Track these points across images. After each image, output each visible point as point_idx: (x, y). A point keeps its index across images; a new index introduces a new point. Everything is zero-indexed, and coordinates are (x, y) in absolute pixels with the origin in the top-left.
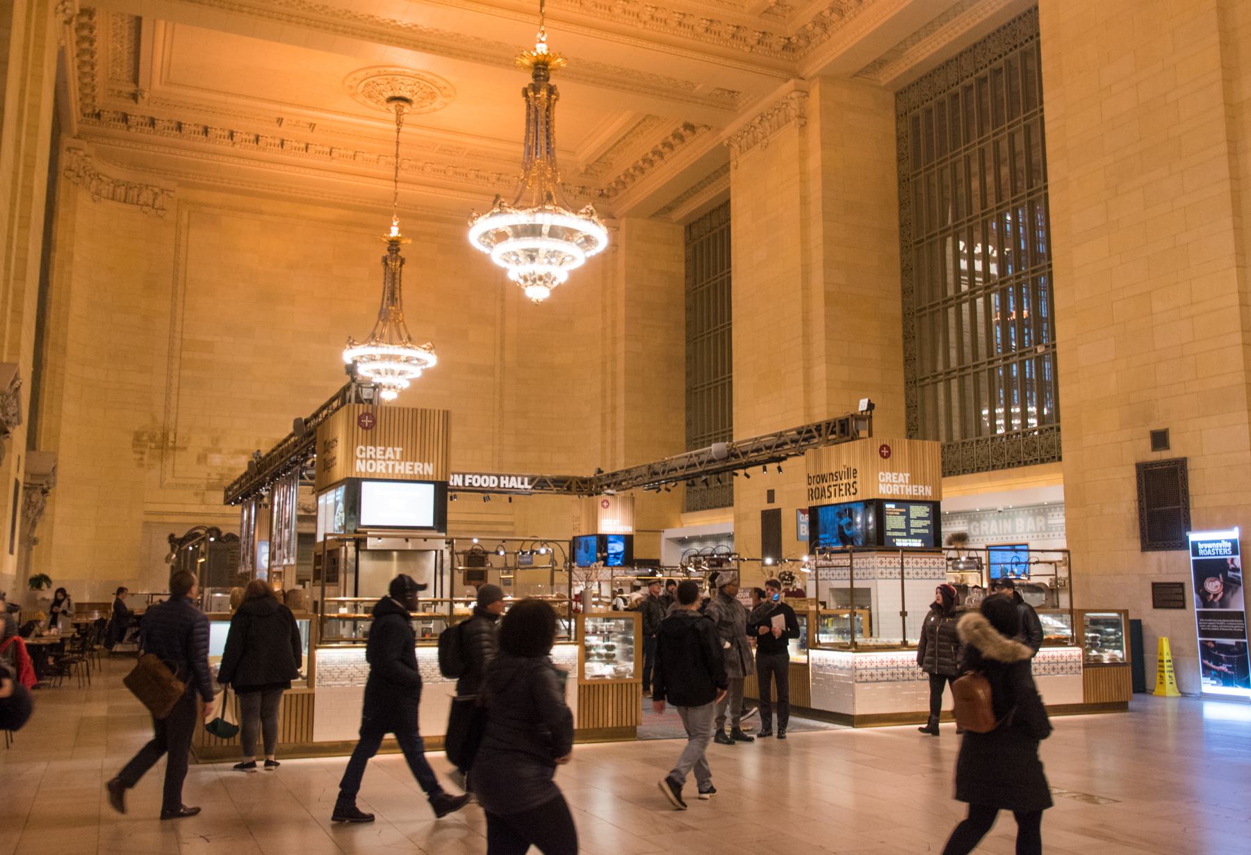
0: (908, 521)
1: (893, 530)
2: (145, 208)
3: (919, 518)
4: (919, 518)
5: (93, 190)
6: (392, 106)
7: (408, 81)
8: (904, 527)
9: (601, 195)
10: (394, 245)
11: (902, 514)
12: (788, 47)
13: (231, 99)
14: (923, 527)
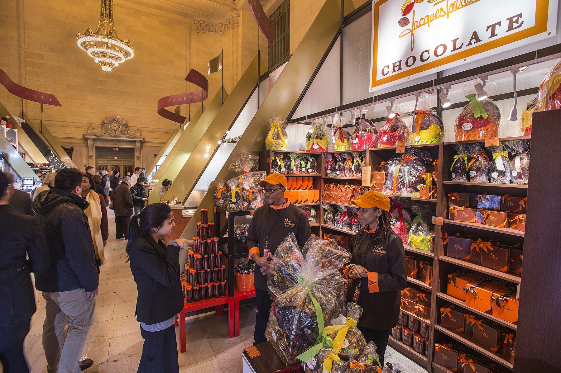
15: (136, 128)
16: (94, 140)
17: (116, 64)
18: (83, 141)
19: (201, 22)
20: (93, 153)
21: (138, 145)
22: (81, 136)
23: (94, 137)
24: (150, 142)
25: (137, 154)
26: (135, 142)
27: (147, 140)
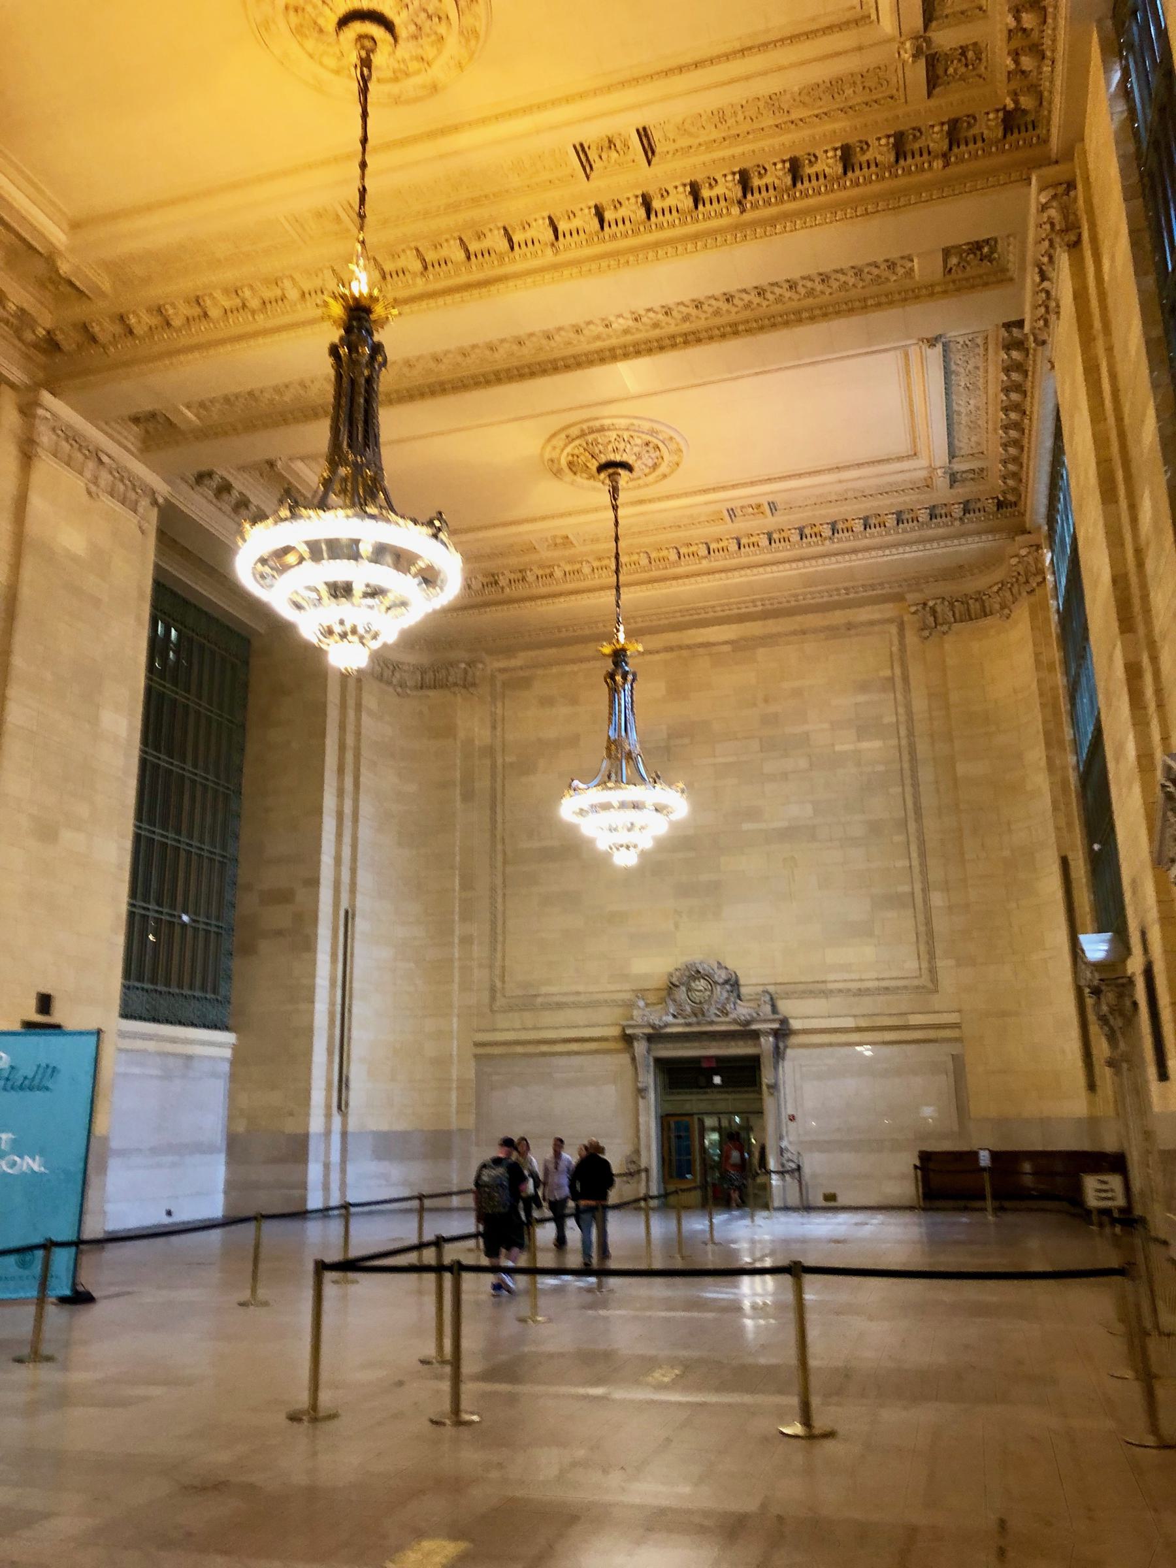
2: (456, 689)
5: (395, 681)
12: (1011, 121)
15: (760, 989)
16: (650, 1038)
17: (647, 843)
18: (620, 1045)
19: (931, 603)
20: (648, 1079)
21: (768, 1042)
22: (615, 1031)
23: (650, 1031)
24: (806, 1032)
25: (767, 1078)
26: (755, 1035)
27: (795, 1024)
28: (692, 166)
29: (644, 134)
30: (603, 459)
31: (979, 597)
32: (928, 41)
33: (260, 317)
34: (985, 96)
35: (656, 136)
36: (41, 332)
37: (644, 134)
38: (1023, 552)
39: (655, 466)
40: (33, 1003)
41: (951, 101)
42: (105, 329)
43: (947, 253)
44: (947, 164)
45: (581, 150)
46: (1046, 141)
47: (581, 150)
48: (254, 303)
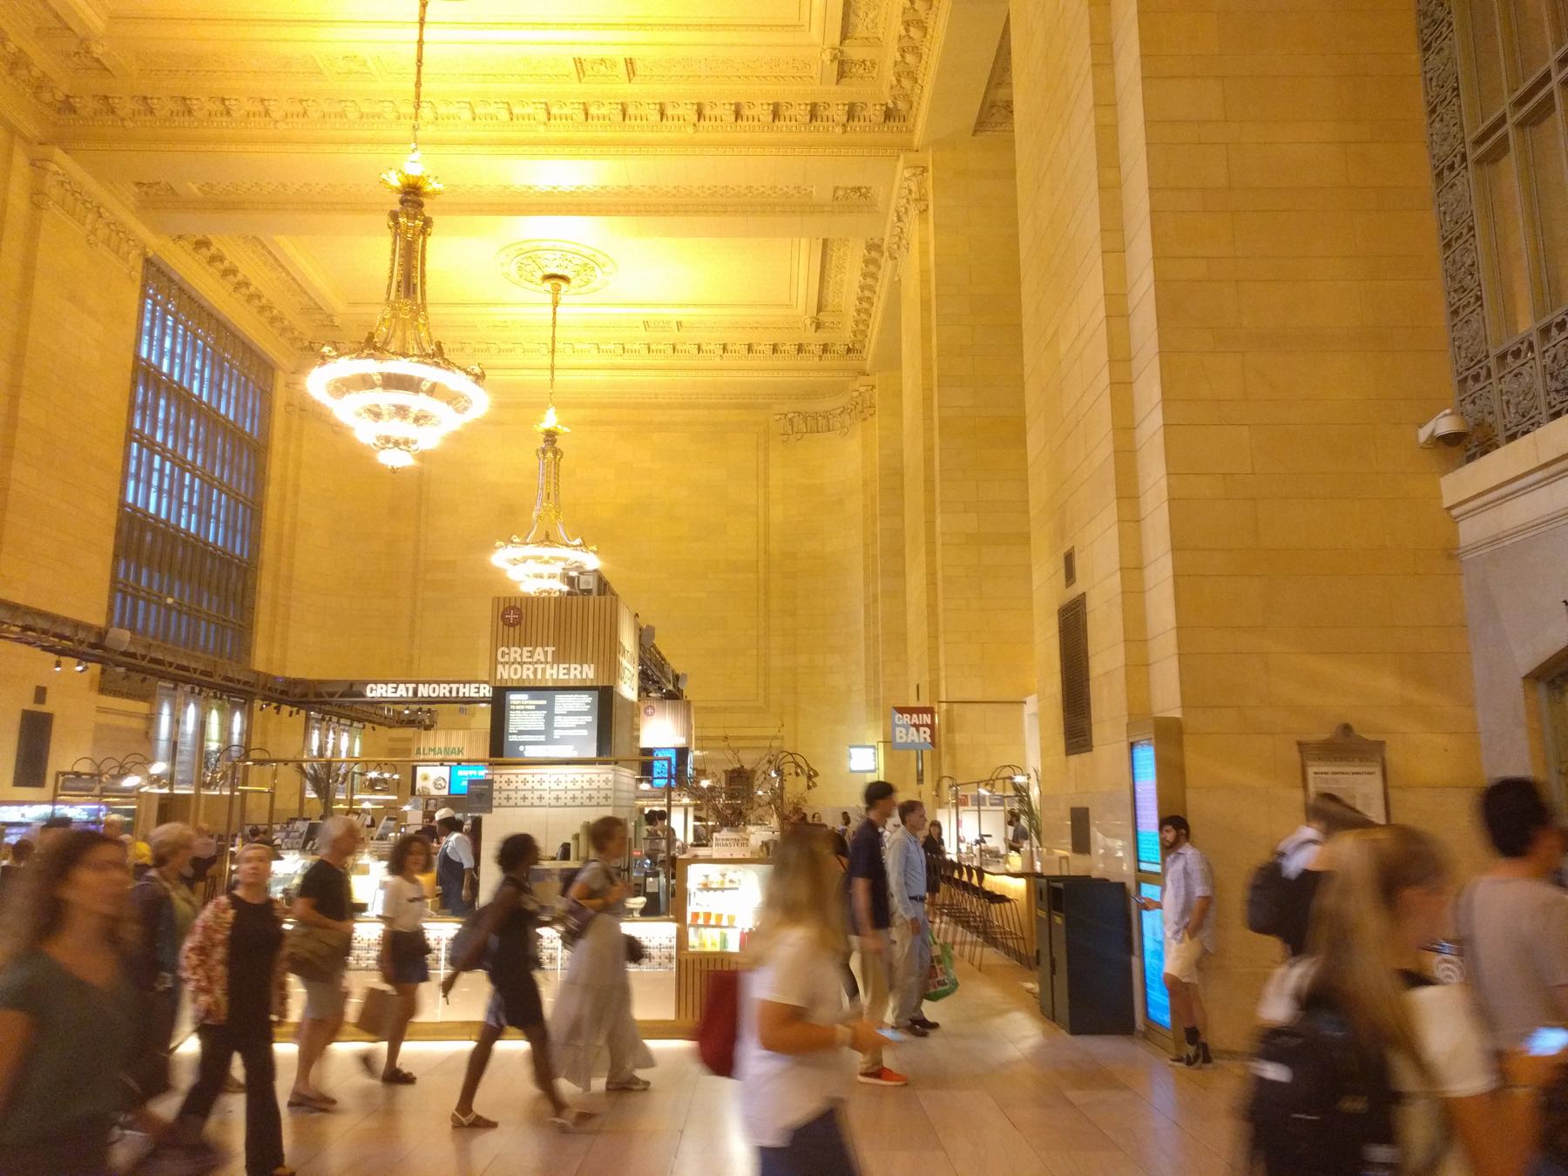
0: (549, 719)
1: (521, 733)
3: (570, 713)
4: (570, 713)
6: (548, 285)
7: (549, 255)
8: (542, 727)
9: (849, 350)
10: (551, 436)
11: (539, 708)
12: (889, 115)
13: (454, 310)
14: (579, 727)
28: (663, 90)
29: (630, 63)
30: (548, 271)
31: (826, 416)
32: (842, 52)
33: (282, 126)
34: (877, 90)
35: (638, 64)
36: (60, 96)
37: (630, 63)
38: (862, 389)
39: (588, 282)
40: (30, 694)
41: (852, 90)
42: (127, 107)
43: (836, 189)
44: (845, 132)
45: (578, 62)
46: (910, 131)
47: (578, 62)
48: (276, 115)
